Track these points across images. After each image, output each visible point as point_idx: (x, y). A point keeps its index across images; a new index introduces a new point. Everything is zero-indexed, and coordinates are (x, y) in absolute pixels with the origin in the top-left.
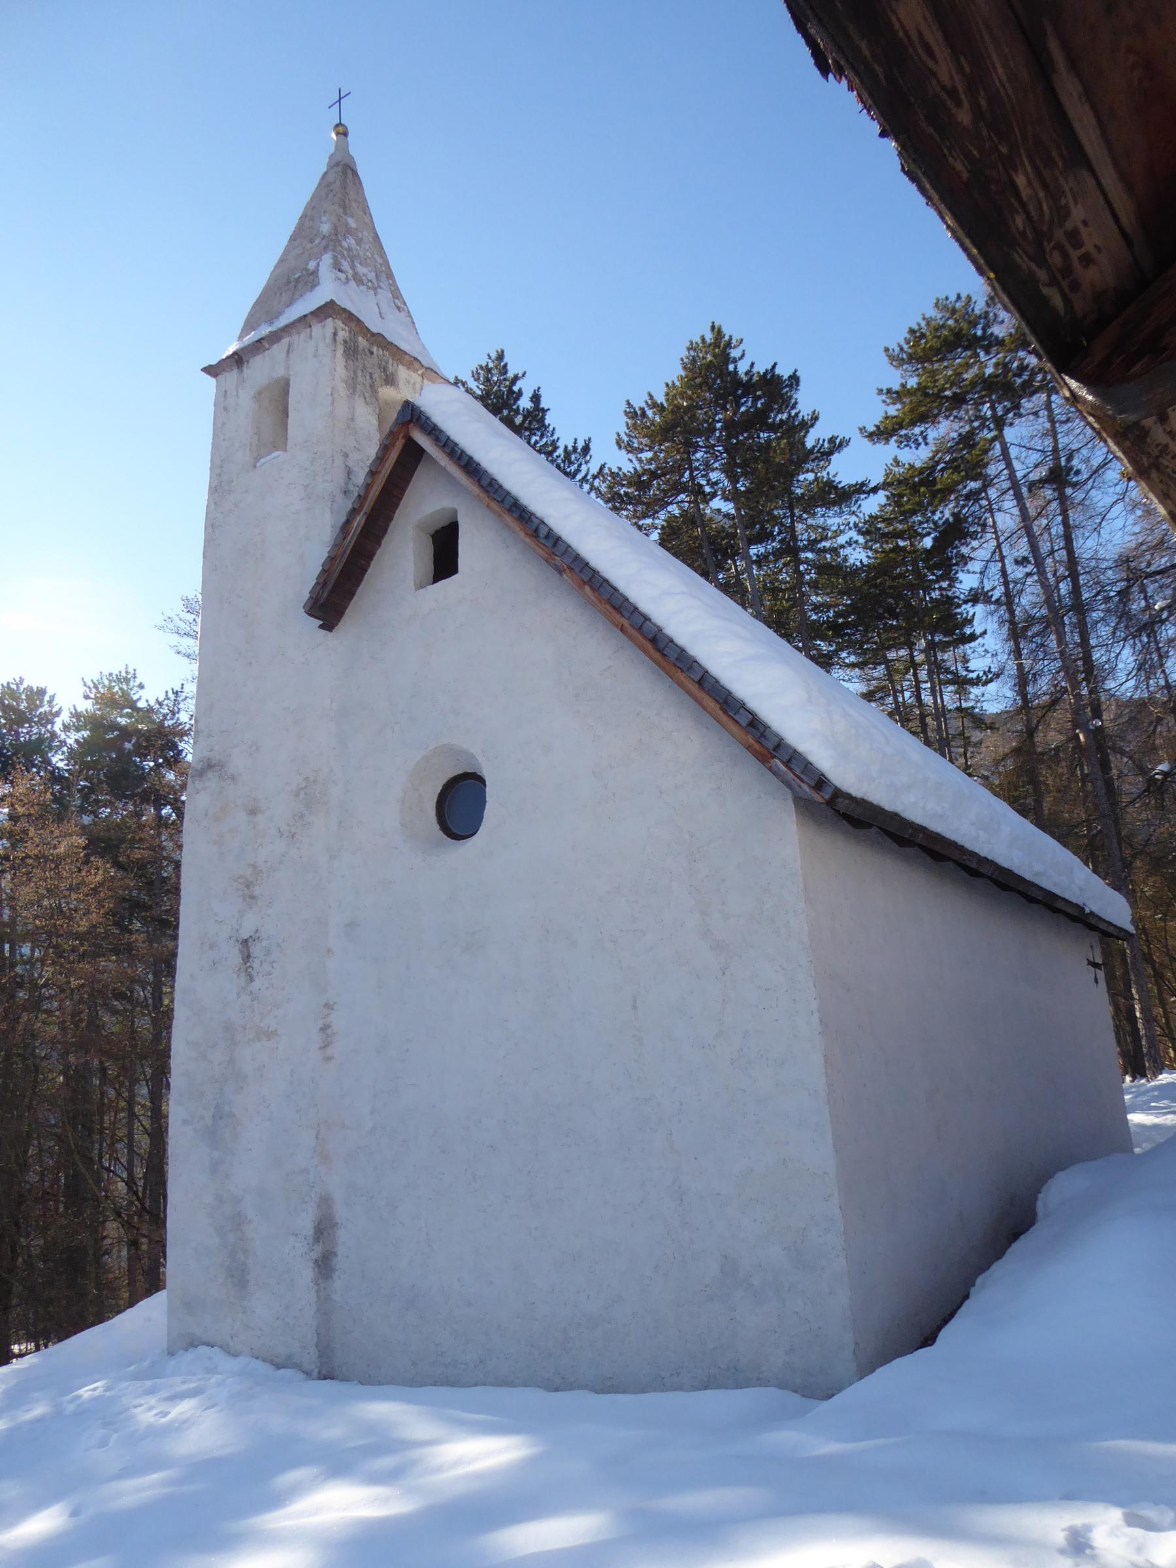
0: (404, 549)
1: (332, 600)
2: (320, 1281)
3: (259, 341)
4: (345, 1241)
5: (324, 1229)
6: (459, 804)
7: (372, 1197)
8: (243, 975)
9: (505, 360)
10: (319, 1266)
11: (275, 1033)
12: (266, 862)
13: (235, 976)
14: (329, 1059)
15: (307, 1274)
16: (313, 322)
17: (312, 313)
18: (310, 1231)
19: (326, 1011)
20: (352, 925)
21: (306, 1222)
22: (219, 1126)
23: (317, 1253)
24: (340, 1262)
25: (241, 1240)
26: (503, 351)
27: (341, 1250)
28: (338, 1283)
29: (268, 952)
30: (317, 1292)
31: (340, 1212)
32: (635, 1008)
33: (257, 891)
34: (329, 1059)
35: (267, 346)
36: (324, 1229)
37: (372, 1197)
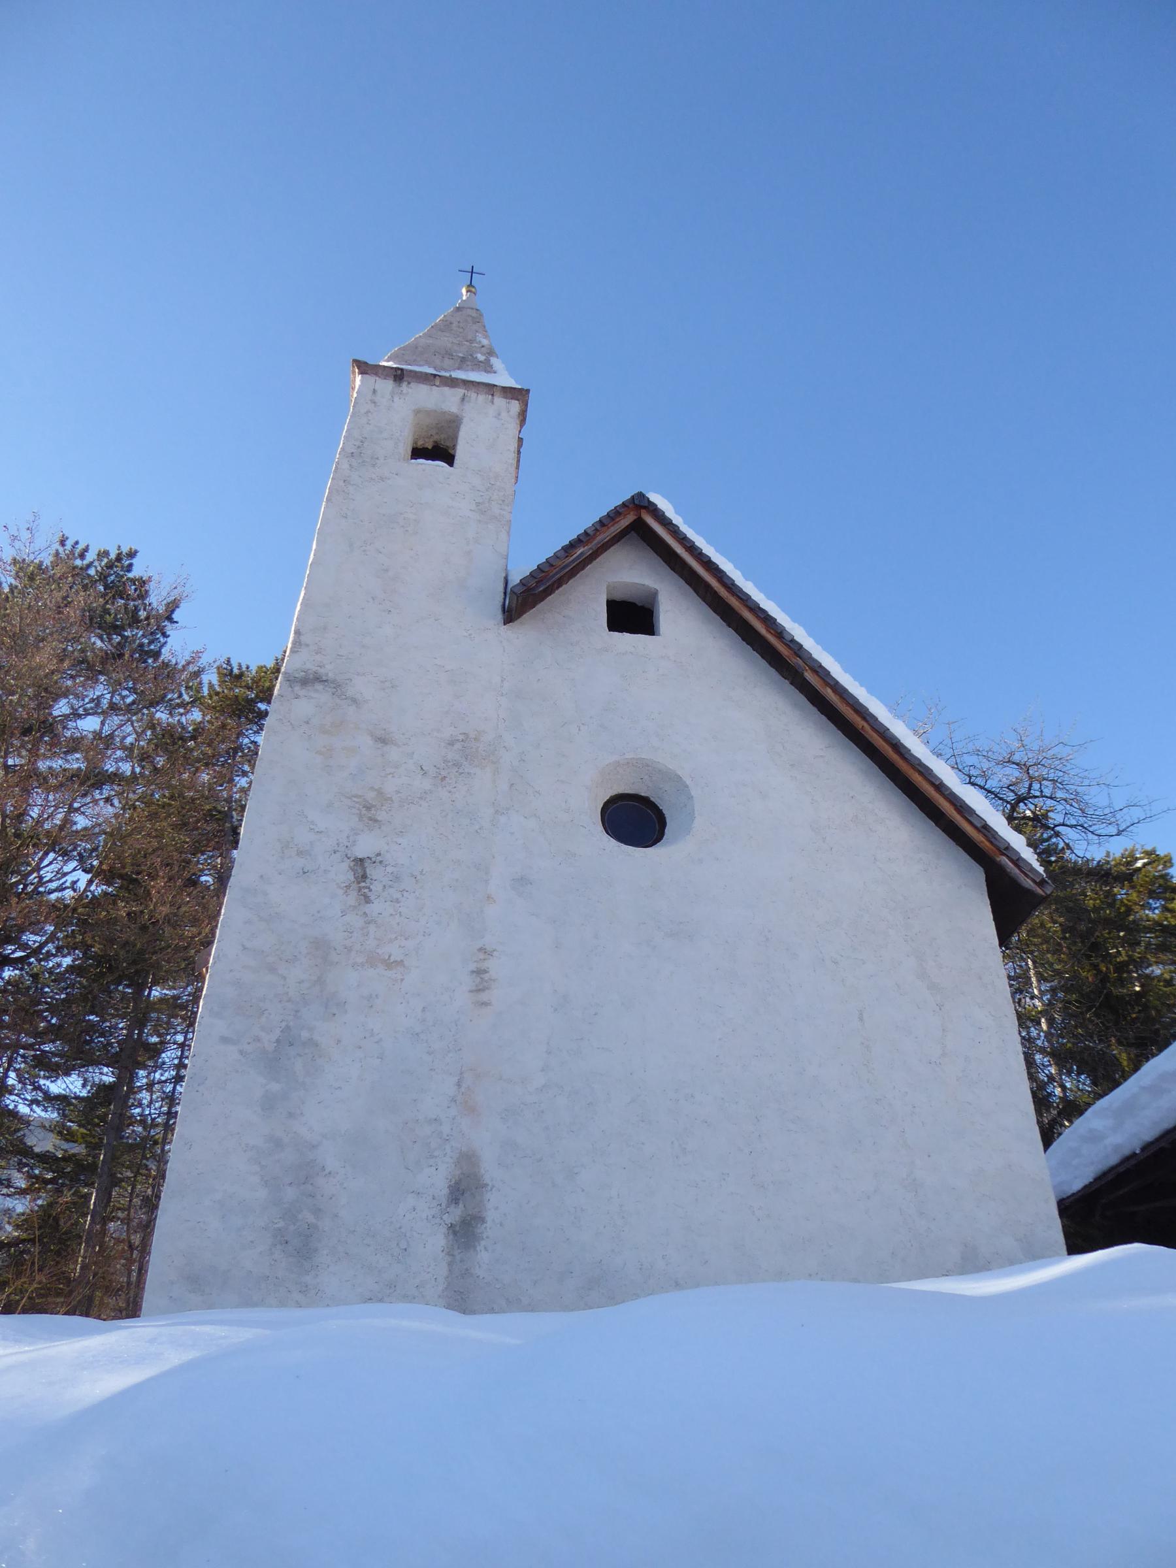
0: (587, 601)
1: (524, 600)
2: (456, 1252)
3: (435, 376)
4: (498, 1207)
5: (465, 1189)
6: (635, 819)
7: (540, 1160)
8: (353, 894)
9: (134, 561)
10: (455, 1233)
11: (400, 963)
12: (398, 792)
13: (341, 892)
14: (485, 1004)
15: (437, 1241)
16: (497, 394)
17: (504, 388)
18: (443, 1191)
19: (482, 956)
20: (521, 882)
21: (438, 1179)
22: (286, 1055)
23: (455, 1214)
24: (490, 1230)
25: (312, 1196)
26: (136, 552)
27: (491, 1215)
28: (483, 1258)
29: (397, 878)
30: (450, 1264)
31: (490, 1170)
32: (861, 1019)
33: (381, 815)
34: (485, 1004)
35: (438, 383)
36: (465, 1189)
37: (540, 1160)
